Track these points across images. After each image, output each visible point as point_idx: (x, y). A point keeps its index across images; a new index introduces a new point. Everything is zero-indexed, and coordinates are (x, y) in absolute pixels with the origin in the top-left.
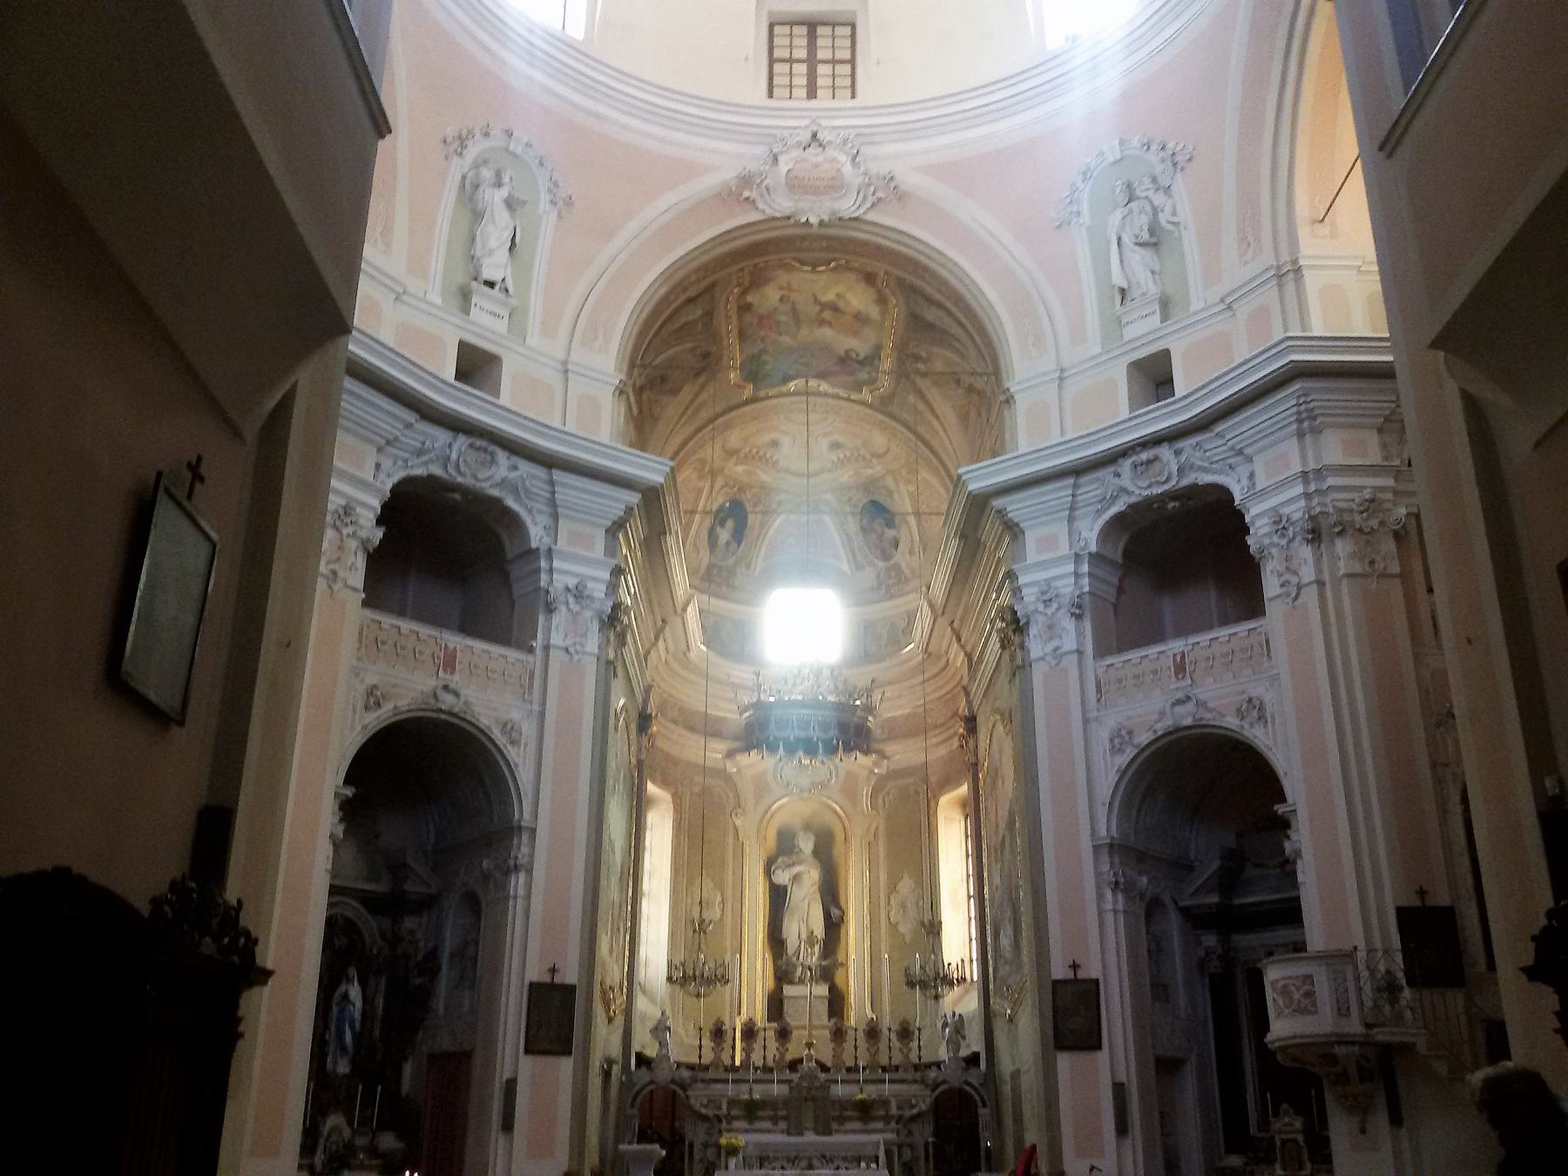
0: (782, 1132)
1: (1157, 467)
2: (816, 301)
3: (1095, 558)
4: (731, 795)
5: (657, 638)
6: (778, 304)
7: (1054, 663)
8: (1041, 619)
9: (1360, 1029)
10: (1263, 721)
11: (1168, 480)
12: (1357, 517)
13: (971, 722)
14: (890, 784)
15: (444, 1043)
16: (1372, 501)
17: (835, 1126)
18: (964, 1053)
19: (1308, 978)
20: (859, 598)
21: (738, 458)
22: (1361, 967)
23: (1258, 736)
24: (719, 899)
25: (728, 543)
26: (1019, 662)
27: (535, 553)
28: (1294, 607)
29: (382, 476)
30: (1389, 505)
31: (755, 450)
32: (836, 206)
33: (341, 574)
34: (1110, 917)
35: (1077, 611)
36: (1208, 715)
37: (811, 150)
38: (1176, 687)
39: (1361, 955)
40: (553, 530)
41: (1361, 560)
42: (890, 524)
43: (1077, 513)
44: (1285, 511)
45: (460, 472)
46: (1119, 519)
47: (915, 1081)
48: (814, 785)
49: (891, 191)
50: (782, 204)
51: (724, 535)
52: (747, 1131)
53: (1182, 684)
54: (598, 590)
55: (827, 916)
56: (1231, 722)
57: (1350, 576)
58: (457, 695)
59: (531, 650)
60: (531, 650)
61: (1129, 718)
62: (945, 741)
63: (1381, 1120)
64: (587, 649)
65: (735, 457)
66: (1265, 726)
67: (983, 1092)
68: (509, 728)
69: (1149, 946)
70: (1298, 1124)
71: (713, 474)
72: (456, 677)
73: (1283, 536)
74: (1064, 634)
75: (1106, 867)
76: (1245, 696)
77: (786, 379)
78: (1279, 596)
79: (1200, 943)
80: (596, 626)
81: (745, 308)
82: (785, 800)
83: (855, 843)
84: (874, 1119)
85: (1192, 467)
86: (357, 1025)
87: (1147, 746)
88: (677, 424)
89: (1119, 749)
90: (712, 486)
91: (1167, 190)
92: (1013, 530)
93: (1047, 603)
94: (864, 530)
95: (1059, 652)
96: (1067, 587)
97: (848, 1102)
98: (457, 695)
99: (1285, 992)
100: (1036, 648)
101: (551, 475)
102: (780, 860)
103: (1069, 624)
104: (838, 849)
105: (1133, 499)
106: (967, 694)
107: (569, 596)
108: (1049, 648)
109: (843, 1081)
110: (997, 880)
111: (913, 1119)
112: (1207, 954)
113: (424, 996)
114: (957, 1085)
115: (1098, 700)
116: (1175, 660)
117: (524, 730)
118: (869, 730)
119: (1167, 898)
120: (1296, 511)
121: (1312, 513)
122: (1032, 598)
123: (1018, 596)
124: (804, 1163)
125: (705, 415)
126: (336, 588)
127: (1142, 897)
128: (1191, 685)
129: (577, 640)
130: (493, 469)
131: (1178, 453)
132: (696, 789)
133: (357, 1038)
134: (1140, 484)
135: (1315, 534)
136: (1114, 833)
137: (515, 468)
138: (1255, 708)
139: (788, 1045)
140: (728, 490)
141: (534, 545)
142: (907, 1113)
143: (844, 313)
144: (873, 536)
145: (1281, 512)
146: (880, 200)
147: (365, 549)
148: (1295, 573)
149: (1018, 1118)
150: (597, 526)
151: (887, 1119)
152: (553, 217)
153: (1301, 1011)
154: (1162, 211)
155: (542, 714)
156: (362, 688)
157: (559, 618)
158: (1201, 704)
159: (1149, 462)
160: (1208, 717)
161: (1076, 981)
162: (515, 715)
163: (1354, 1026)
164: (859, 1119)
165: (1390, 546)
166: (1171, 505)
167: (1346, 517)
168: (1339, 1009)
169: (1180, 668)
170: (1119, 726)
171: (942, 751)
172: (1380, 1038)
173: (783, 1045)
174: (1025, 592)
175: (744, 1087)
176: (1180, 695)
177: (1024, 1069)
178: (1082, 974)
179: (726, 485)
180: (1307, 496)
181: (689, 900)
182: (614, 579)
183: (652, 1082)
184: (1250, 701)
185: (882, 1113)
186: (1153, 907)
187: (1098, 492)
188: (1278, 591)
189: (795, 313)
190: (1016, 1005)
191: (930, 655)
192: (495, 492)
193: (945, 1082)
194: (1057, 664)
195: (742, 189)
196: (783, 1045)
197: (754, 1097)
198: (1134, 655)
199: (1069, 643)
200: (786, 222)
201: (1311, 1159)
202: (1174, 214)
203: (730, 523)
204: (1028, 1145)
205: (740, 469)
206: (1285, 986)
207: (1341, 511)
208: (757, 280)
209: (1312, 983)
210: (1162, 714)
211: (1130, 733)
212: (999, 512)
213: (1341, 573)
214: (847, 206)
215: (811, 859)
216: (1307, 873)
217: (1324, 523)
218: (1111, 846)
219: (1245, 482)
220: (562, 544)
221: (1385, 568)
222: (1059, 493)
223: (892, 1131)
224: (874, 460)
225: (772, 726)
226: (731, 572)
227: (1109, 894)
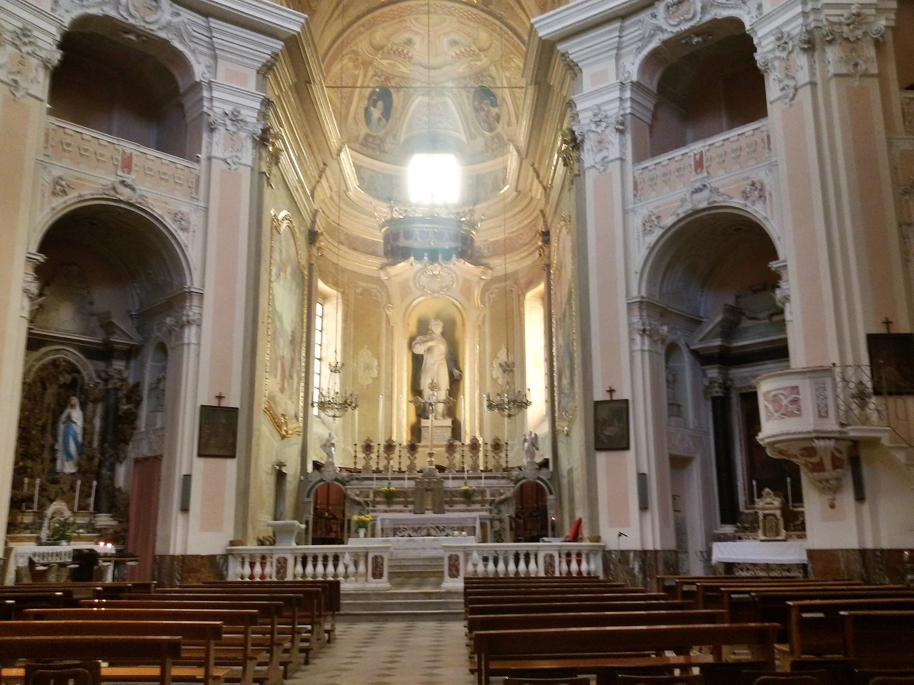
0: (410, 511)
3: (636, 86)
4: (383, 294)
5: (320, 177)
7: (602, 168)
8: (592, 135)
9: (836, 428)
10: (762, 199)
11: (691, 19)
12: (845, 29)
13: (546, 235)
14: (493, 286)
15: (145, 451)
16: (858, 15)
17: (447, 507)
18: (538, 460)
19: (795, 389)
20: (470, 158)
22: (838, 379)
23: (758, 211)
24: (376, 363)
25: (379, 119)
26: (576, 172)
27: (197, 86)
28: (791, 105)
29: (61, 11)
30: (872, 19)
33: (22, 84)
34: (638, 356)
35: (621, 127)
36: (721, 199)
38: (696, 180)
39: (838, 370)
40: (213, 69)
41: (847, 62)
42: (494, 104)
43: (623, 51)
44: (786, 29)
45: (131, 15)
46: (655, 53)
47: (503, 478)
48: (442, 288)
51: (376, 113)
52: (386, 511)
53: (700, 177)
54: (250, 116)
55: (451, 375)
56: (737, 202)
57: (836, 75)
58: (133, 189)
59: (198, 161)
60: (198, 161)
61: (657, 207)
62: (530, 254)
63: (847, 498)
64: (243, 161)
66: (764, 202)
67: (550, 485)
68: (179, 218)
69: (667, 376)
70: (777, 502)
71: (367, 64)
72: (133, 176)
73: (784, 49)
74: (610, 146)
75: (636, 319)
76: (749, 182)
78: (779, 98)
79: (705, 375)
80: (249, 144)
82: (422, 298)
83: (469, 326)
84: (474, 503)
85: (712, 5)
86: (80, 438)
87: (670, 228)
88: (330, 18)
89: (650, 231)
90: (365, 76)
92: (573, 69)
93: (598, 123)
94: (476, 110)
95: (606, 160)
96: (613, 110)
97: (456, 491)
98: (133, 189)
99: (775, 400)
100: (589, 157)
101: (208, 22)
102: (418, 338)
103: (614, 138)
104: (458, 333)
105: (666, 36)
106: (544, 216)
107: (226, 119)
108: (599, 158)
109: (453, 478)
110: (561, 341)
111: (502, 502)
112: (711, 383)
113: (131, 418)
114: (531, 480)
115: (635, 196)
116: (695, 159)
117: (191, 220)
118: (472, 240)
119: (682, 344)
120: (796, 29)
121: (808, 28)
122: (587, 121)
123: (576, 119)
124: (424, 532)
125: (353, 12)
126: (18, 95)
127: (663, 341)
128: (707, 177)
129: (235, 153)
130: (159, 13)
132: (359, 290)
133: (80, 447)
135: (810, 45)
136: (644, 293)
137: (178, 14)
138: (758, 190)
139: (417, 455)
140: (377, 78)
141: (197, 79)
142: (498, 499)
144: (483, 113)
145: (783, 30)
147: (46, 67)
148: (793, 78)
149: (572, 501)
151: (483, 503)
153: (788, 414)
155: (206, 209)
156: (48, 179)
157: (219, 136)
158: (715, 191)
160: (720, 200)
161: (612, 401)
162: (184, 209)
163: (831, 425)
164: (463, 503)
165: (871, 52)
166: (695, 40)
167: (836, 29)
168: (819, 411)
169: (699, 164)
170: (651, 213)
171: (528, 262)
172: (852, 434)
173: (412, 455)
174: (581, 116)
175: (385, 483)
176: (698, 185)
177: (575, 467)
178: (616, 397)
179: (375, 75)
180: (805, 14)
181: (355, 365)
182: (263, 109)
183: (322, 480)
184: (753, 184)
185: (479, 498)
186: (671, 350)
187: (640, 32)
188: (780, 94)
190: (571, 422)
191: (519, 192)
192: (162, 34)
193: (524, 478)
194: (604, 171)
196: (412, 455)
197: (391, 489)
198: (663, 158)
199: (614, 152)
201: (786, 529)
203: (380, 104)
204: (577, 518)
205: (384, 62)
206: (775, 396)
207: (832, 24)
209: (798, 393)
210: (683, 200)
211: (658, 218)
212: (563, 55)
213: (830, 75)
215: (440, 338)
216: (793, 314)
217: (817, 35)
218: (641, 302)
219: (754, 13)
220: (221, 79)
221: (866, 69)
222: (607, 36)
223: (486, 511)
224: (482, 53)
225: (401, 235)
226: (382, 140)
227: (638, 338)
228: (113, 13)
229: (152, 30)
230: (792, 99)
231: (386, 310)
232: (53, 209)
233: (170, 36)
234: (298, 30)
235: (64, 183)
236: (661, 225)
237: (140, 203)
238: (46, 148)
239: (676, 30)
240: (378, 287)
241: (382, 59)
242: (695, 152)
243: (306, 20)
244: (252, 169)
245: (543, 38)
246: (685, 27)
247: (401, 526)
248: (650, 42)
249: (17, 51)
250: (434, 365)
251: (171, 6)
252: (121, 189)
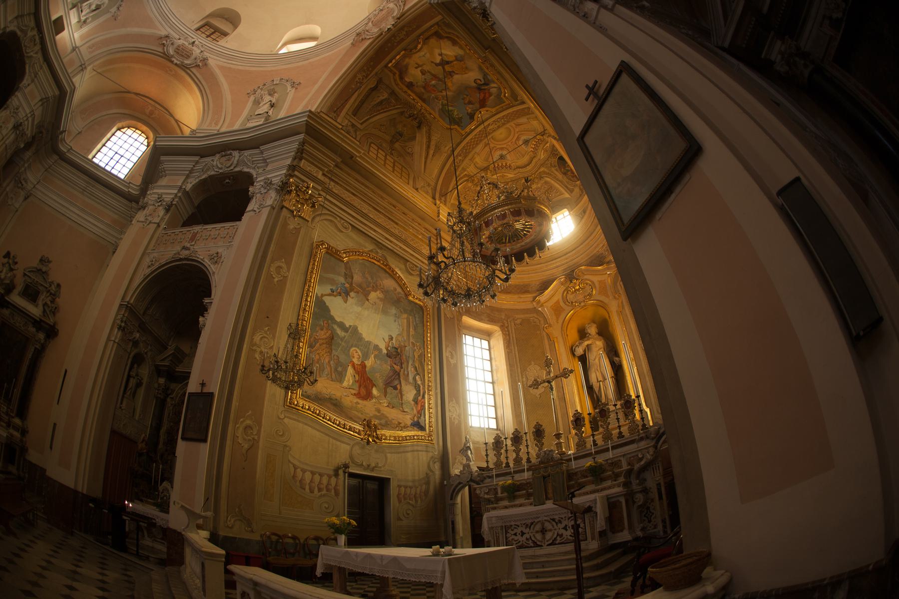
0: (531, 504)
2: (437, 65)
4: (540, 319)
55: (613, 364)
77: (472, 117)
81: (410, 85)
84: (603, 480)
88: (426, 158)
111: (644, 469)
132: (518, 322)
142: (637, 467)
143: (452, 62)
144: (569, 173)
189: (435, 77)
192: (237, 169)
200: (382, 36)
208: (402, 70)
231: (545, 329)
240: (535, 315)
241: (492, 175)
247: (513, 523)
250: (595, 360)
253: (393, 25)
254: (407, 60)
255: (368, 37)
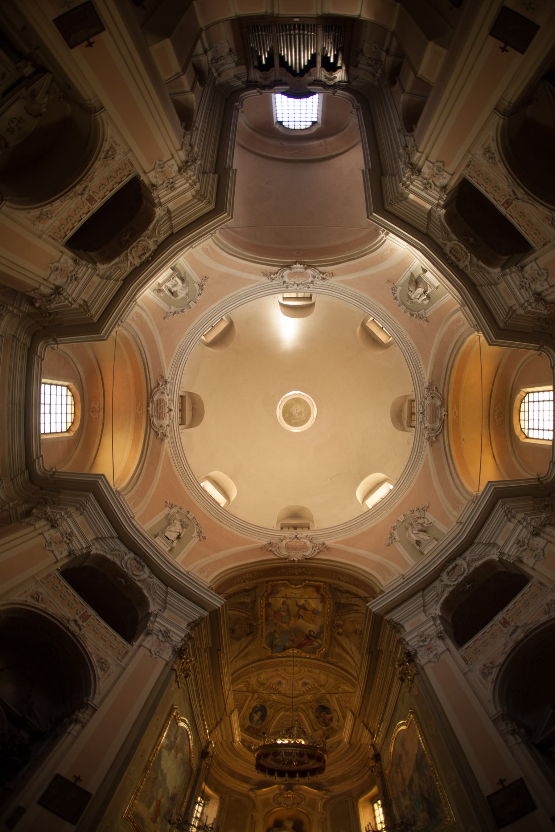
1: (457, 569)
6: (281, 605)
7: (436, 660)
11: (463, 573)
21: (264, 687)
31: (271, 686)
32: (305, 553)
37: (295, 540)
43: (427, 608)
45: (127, 567)
49: (325, 548)
50: (284, 553)
58: (80, 629)
60: (132, 645)
65: (263, 687)
68: (103, 664)
72: (84, 624)
91: (424, 518)
93: (423, 641)
98: (80, 629)
105: (451, 588)
108: (431, 656)
126: (47, 548)
130: (142, 573)
131: (464, 559)
134: (453, 580)
146: (321, 551)
150: (185, 620)
152: (198, 539)
154: (425, 523)
155: (124, 669)
159: (454, 568)
187: (435, 592)
195: (268, 548)
200: (284, 561)
202: (428, 521)
208: (273, 592)
210: (505, 645)
214: (308, 553)
228: (118, 563)
229: (135, 580)
230: (544, 555)
232: (26, 601)
233: (143, 587)
234: (220, 606)
235: (41, 596)
236: (497, 664)
237: (81, 638)
238: (44, 578)
239: (456, 583)
242: (499, 620)
243: (225, 603)
244: (167, 664)
245: (376, 612)
246: (460, 579)
248: (442, 595)
249: (62, 538)
251: (150, 573)
252: (72, 623)
253: (299, 560)
254: (283, 588)
255: (276, 553)
